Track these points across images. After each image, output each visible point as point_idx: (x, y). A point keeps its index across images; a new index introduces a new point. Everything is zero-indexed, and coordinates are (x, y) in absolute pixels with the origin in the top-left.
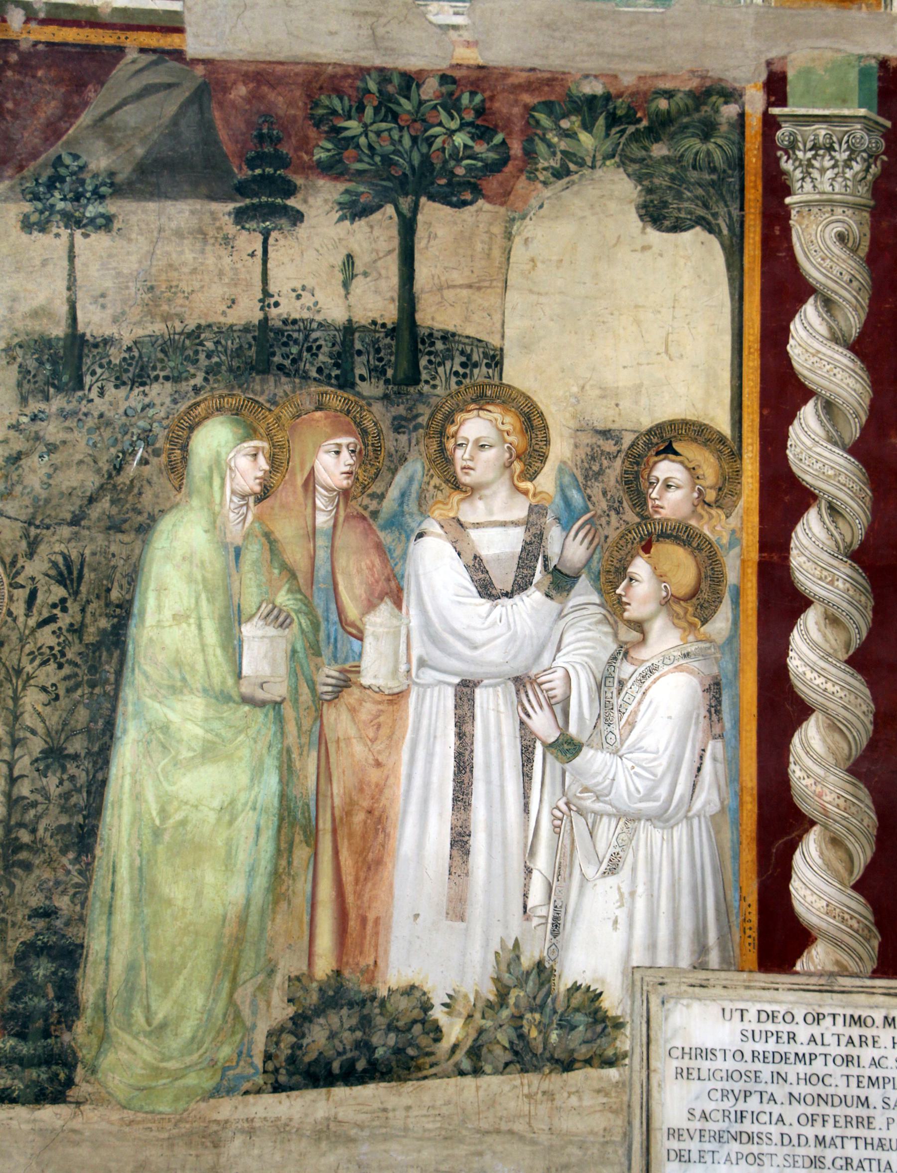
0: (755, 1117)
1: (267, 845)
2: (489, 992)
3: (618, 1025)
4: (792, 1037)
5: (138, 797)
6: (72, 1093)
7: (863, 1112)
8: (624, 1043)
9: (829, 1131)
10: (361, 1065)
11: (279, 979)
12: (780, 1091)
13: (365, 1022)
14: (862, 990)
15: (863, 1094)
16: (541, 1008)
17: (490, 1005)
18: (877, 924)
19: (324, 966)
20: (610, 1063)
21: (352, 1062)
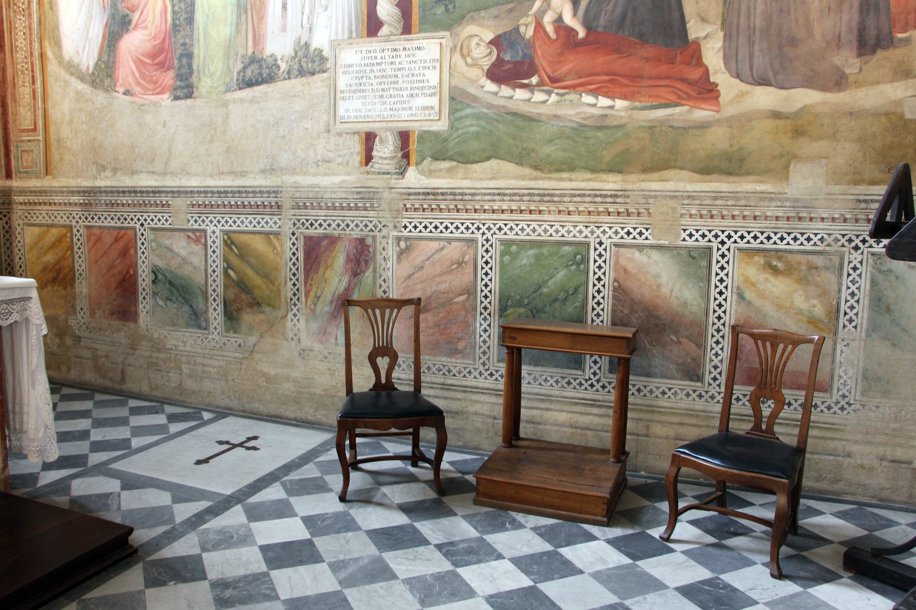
0: (365, 84)
1: (235, 16)
2: (293, 54)
3: (327, 59)
4: (376, 58)
5: (203, 6)
6: (194, 95)
7: (396, 79)
8: (329, 65)
9: (386, 87)
10: (260, 80)
11: (239, 56)
12: (372, 75)
13: (261, 67)
14: (400, 40)
15: (396, 74)
16: (306, 57)
17: (293, 58)
18: (403, 17)
19: (250, 51)
20: (325, 72)
21: (258, 79)
